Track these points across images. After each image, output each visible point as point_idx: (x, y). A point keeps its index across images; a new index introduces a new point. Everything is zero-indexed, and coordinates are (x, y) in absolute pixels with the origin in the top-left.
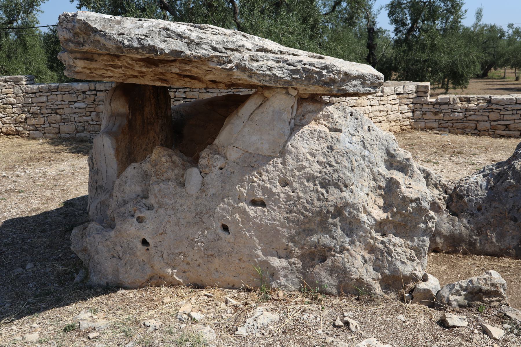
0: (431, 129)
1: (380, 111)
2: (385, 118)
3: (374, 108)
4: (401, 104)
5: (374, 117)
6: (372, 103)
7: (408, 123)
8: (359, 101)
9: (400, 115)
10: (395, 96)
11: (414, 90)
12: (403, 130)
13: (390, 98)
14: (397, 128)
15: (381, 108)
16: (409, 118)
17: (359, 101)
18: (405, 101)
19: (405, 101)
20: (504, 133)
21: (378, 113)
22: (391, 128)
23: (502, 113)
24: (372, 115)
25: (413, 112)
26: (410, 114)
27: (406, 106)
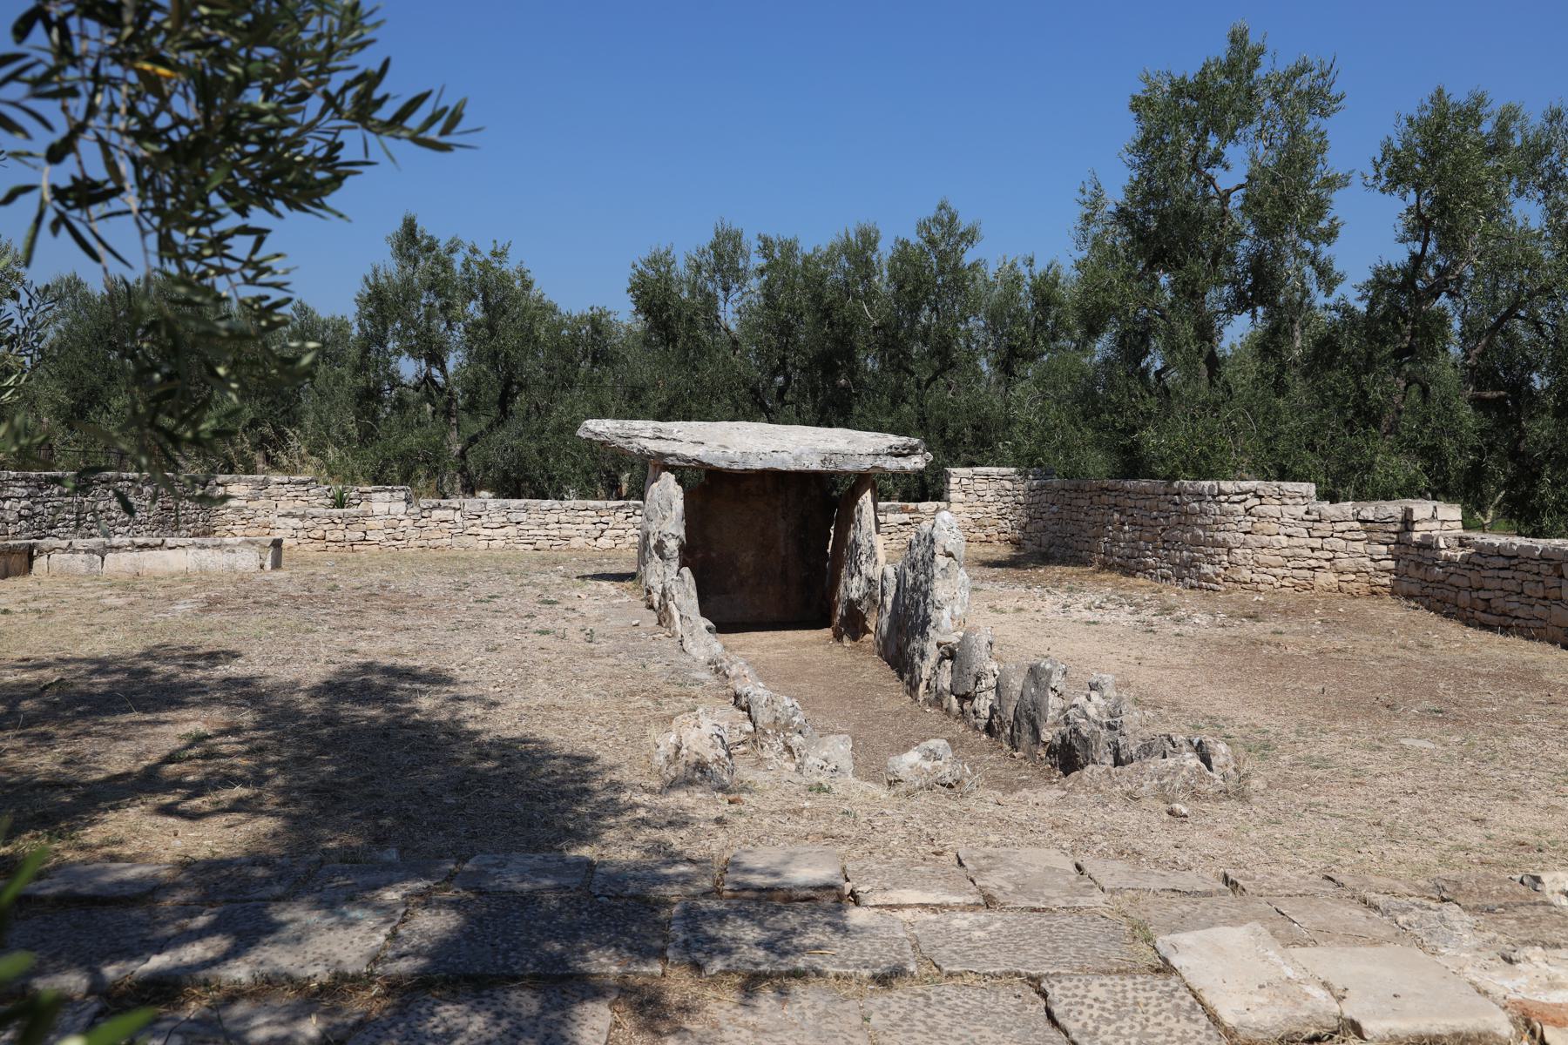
0: (1409, 597)
1: (1313, 550)
2: (1327, 564)
3: (1295, 542)
4: (1370, 541)
5: (1294, 557)
6: (1289, 531)
7: (1386, 581)
8: (1258, 526)
9: (1369, 563)
10: (1357, 525)
11: (1400, 516)
12: (1374, 593)
13: (1340, 527)
14: (1361, 585)
15: (1317, 543)
16: (1388, 571)
17: (1258, 526)
18: (1379, 536)
19: (1379, 536)
20: (1483, 617)
21: (1308, 552)
22: (1344, 585)
23: (1484, 573)
24: (1287, 552)
25: (1396, 559)
26: (1391, 564)
27: (1384, 548)
